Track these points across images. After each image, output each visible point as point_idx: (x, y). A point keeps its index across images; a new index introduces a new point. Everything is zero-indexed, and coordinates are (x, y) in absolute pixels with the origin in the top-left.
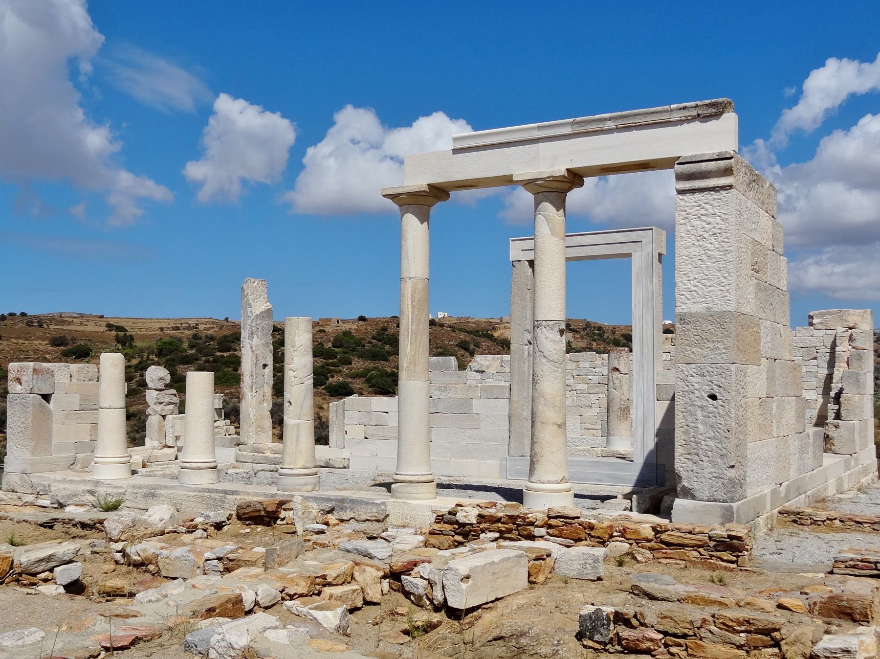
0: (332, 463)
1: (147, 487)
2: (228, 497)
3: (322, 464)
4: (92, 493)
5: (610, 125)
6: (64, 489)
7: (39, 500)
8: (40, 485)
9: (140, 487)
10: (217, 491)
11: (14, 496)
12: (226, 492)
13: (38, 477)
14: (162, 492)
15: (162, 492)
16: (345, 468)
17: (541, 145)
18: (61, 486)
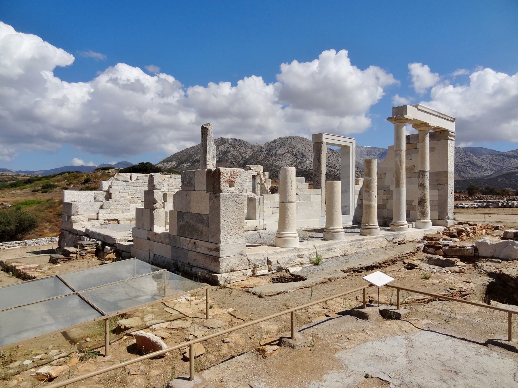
0: (258, 228)
1: (326, 246)
2: (362, 242)
3: (253, 229)
4: (300, 256)
5: (442, 116)
6: (282, 258)
7: (258, 272)
8: (258, 260)
9: (323, 246)
10: (357, 240)
11: (240, 273)
12: (360, 240)
13: (254, 254)
14: (335, 246)
15: (335, 246)
16: (264, 229)
17: (432, 116)
18: (279, 256)
